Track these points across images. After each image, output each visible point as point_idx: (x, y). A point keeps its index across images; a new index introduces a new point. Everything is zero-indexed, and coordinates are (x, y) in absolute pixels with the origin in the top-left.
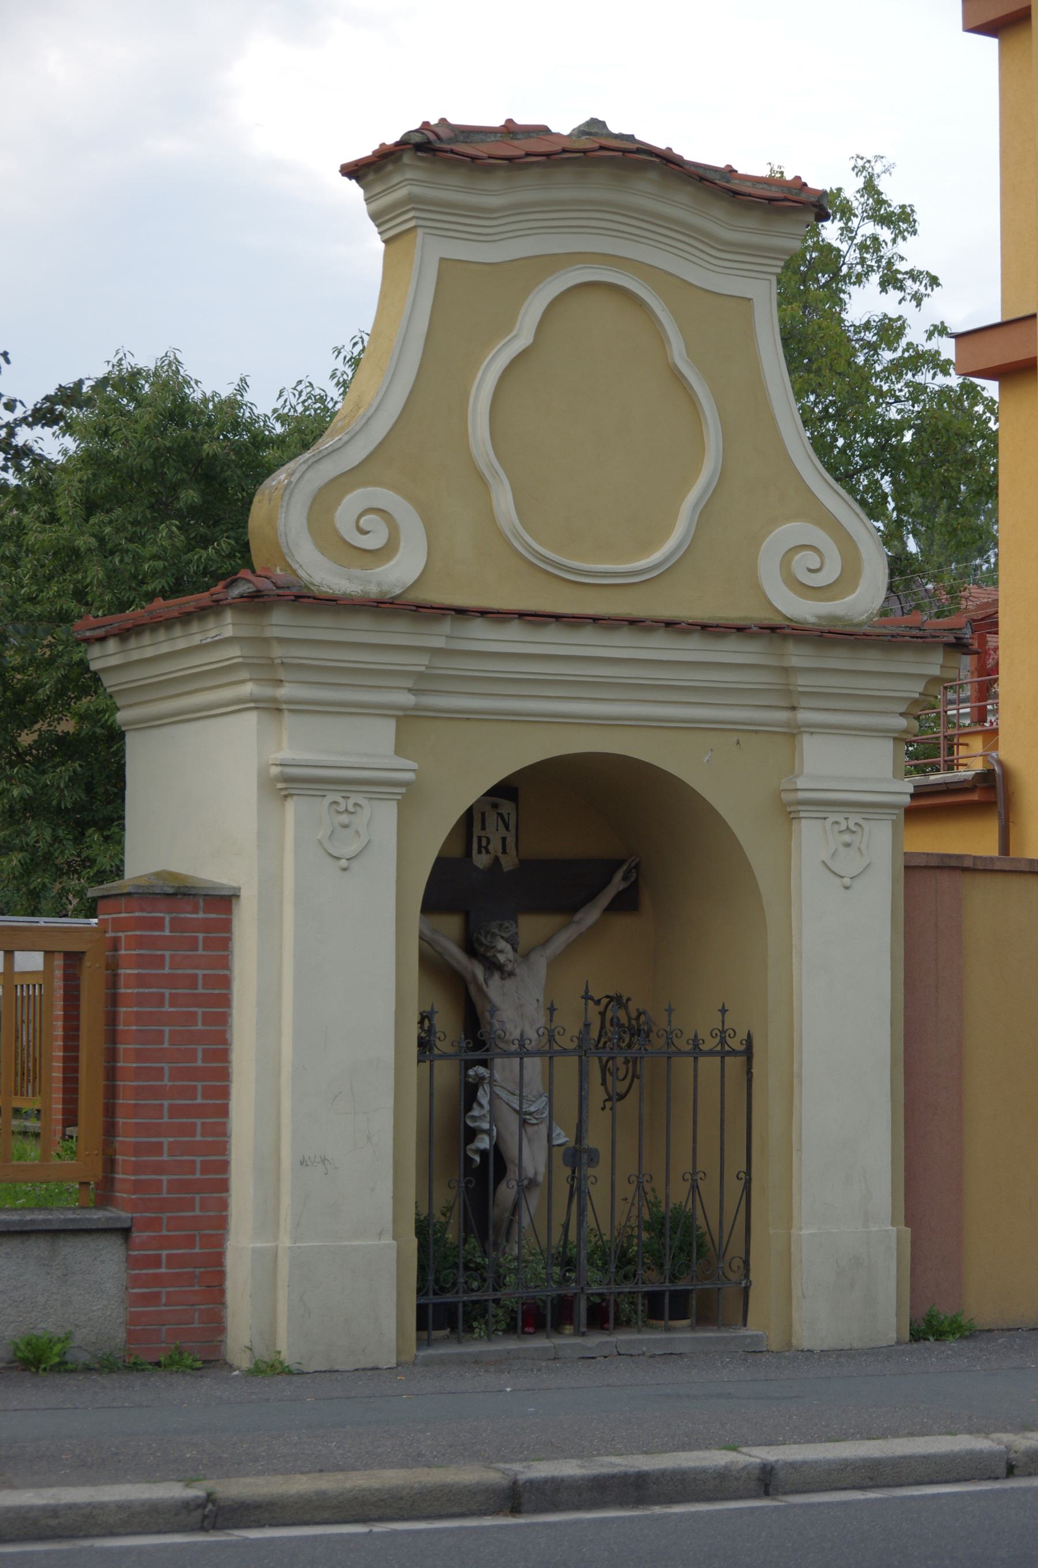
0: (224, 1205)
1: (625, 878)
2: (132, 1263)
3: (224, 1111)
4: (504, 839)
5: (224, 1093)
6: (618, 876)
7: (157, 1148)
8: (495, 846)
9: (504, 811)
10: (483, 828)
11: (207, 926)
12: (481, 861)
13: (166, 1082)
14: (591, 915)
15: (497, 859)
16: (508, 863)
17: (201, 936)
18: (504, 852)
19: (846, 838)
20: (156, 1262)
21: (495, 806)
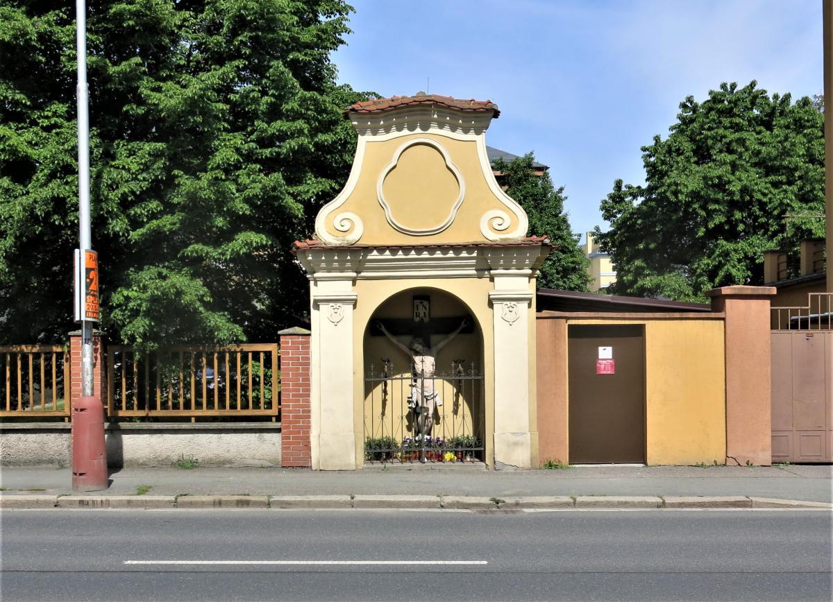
0: (309, 422)
1: (465, 323)
2: (283, 438)
3: (309, 396)
4: (425, 313)
5: (309, 390)
6: (463, 323)
7: (289, 406)
8: (422, 315)
9: (425, 304)
10: (418, 309)
11: (302, 343)
12: (417, 319)
13: (291, 387)
14: (452, 336)
15: (422, 319)
16: (426, 320)
17: (300, 346)
18: (425, 316)
19: (511, 309)
20: (289, 438)
21: (421, 303)
